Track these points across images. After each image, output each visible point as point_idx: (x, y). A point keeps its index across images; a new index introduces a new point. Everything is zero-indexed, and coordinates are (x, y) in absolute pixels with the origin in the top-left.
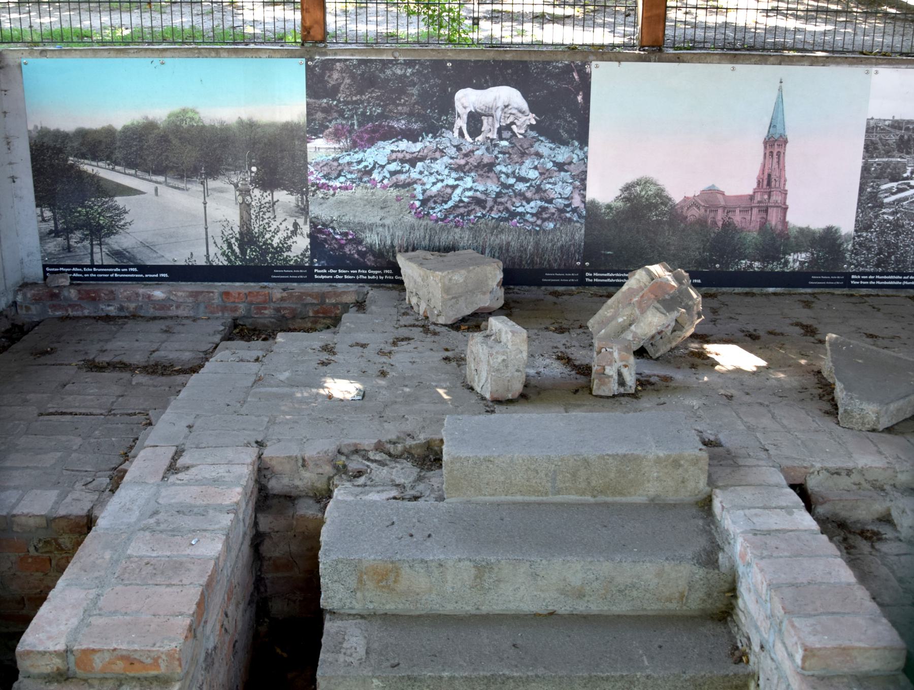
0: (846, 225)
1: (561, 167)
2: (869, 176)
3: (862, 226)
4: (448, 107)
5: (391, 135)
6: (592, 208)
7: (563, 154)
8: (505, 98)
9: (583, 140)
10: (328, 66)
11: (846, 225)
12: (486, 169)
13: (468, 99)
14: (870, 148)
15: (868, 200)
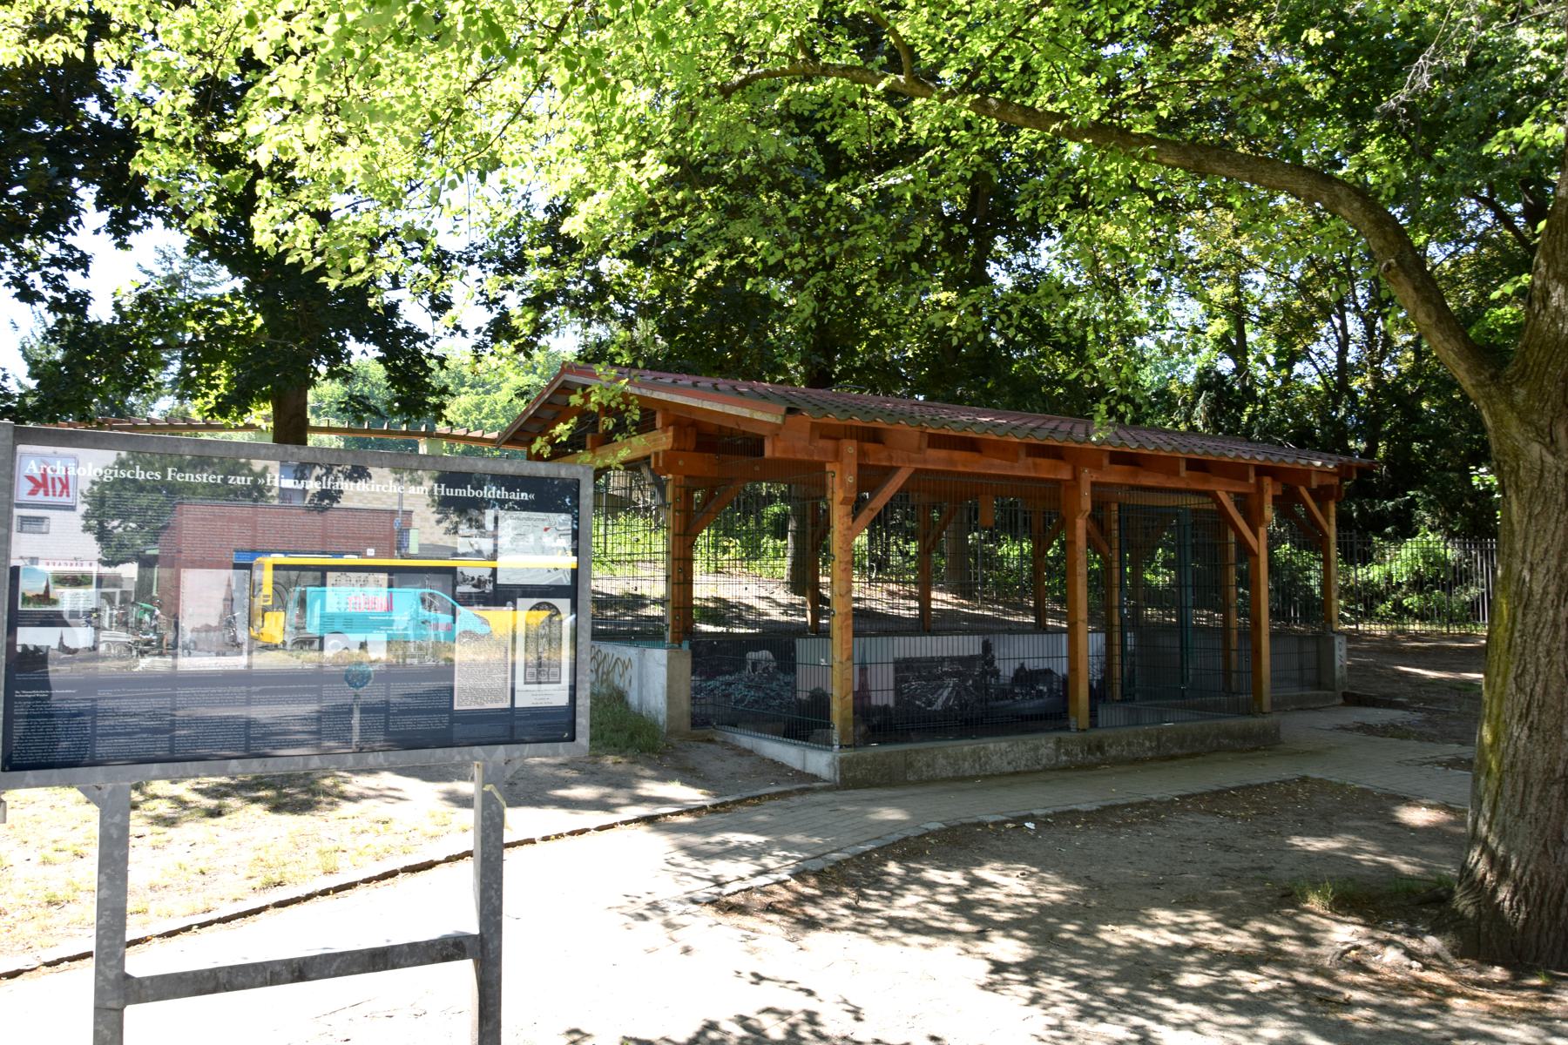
0: (891, 703)
1: (787, 684)
2: (898, 681)
3: (897, 703)
4: (744, 661)
5: (723, 673)
6: (800, 701)
7: (788, 679)
8: (765, 654)
9: (794, 670)
10: (698, 643)
11: (891, 703)
12: (758, 688)
13: (752, 655)
14: (896, 670)
15: (898, 692)
